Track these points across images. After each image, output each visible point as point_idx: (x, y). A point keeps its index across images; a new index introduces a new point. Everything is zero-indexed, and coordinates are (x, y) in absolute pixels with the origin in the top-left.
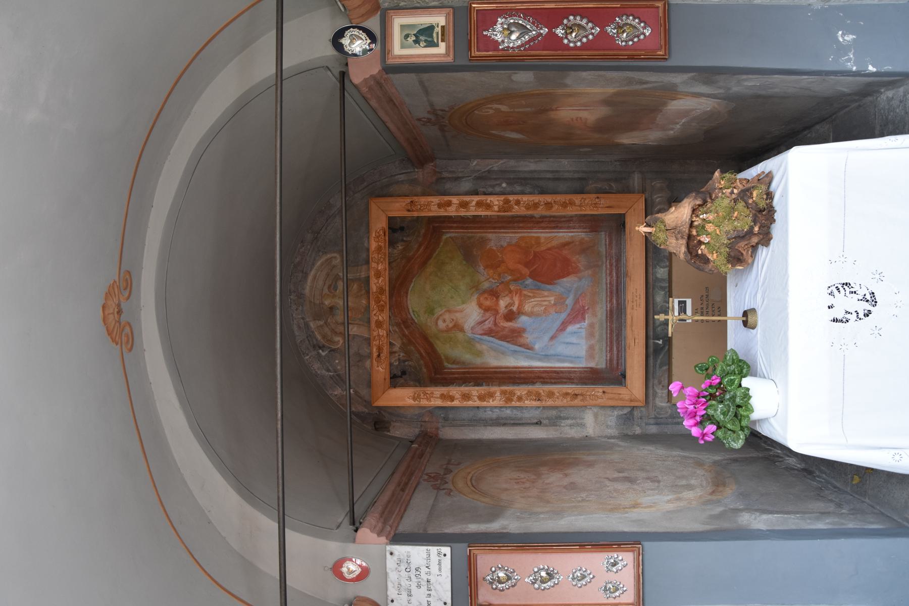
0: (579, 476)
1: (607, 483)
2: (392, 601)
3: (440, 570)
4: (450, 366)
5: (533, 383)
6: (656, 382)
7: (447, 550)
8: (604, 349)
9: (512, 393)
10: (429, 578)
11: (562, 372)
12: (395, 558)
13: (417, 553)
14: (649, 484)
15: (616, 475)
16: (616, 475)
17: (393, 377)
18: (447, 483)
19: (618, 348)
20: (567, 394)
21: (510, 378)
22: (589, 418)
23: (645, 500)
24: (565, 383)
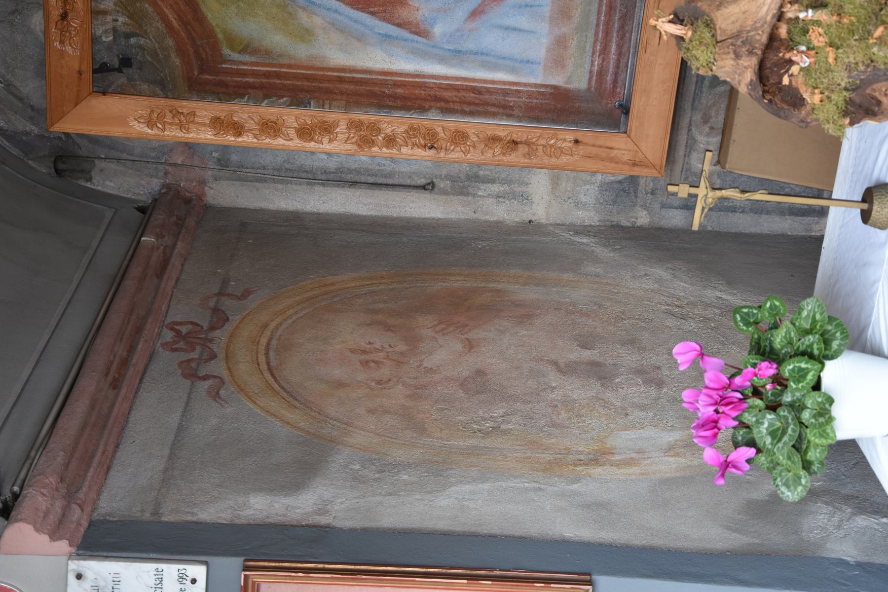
0: (502, 349)
1: (554, 379)
4: (235, 56)
5: (423, 110)
6: (697, 117)
7: (198, 571)
8: (589, 48)
9: (375, 128)
11: (488, 91)
12: (86, 584)
14: (638, 392)
15: (578, 354)
16: (578, 354)
17: (101, 69)
18: (213, 356)
19: (620, 47)
20: (495, 139)
21: (372, 95)
22: (539, 184)
23: (624, 439)
24: (494, 115)
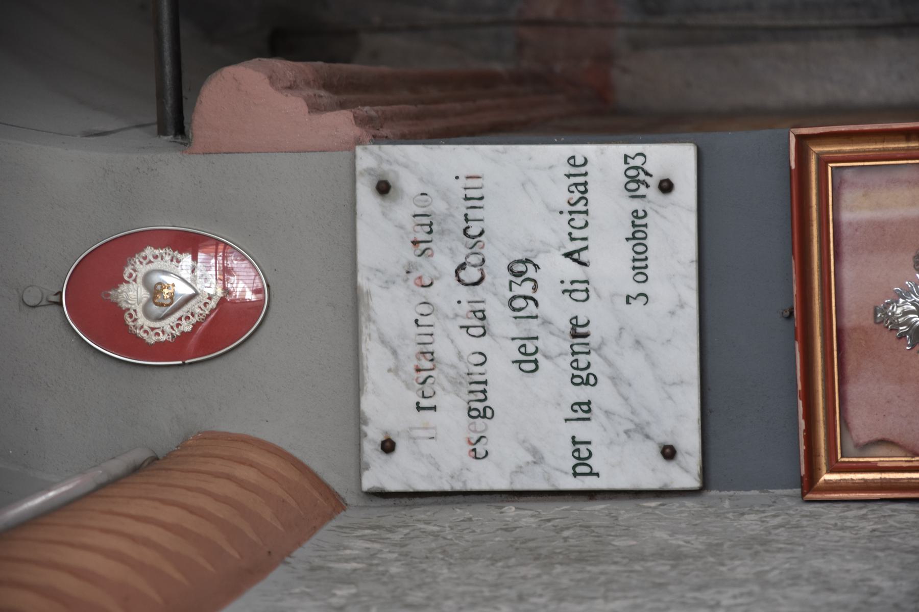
2: (388, 446)
3: (640, 269)
7: (676, 159)
10: (583, 312)
12: (402, 212)
13: (521, 183)
